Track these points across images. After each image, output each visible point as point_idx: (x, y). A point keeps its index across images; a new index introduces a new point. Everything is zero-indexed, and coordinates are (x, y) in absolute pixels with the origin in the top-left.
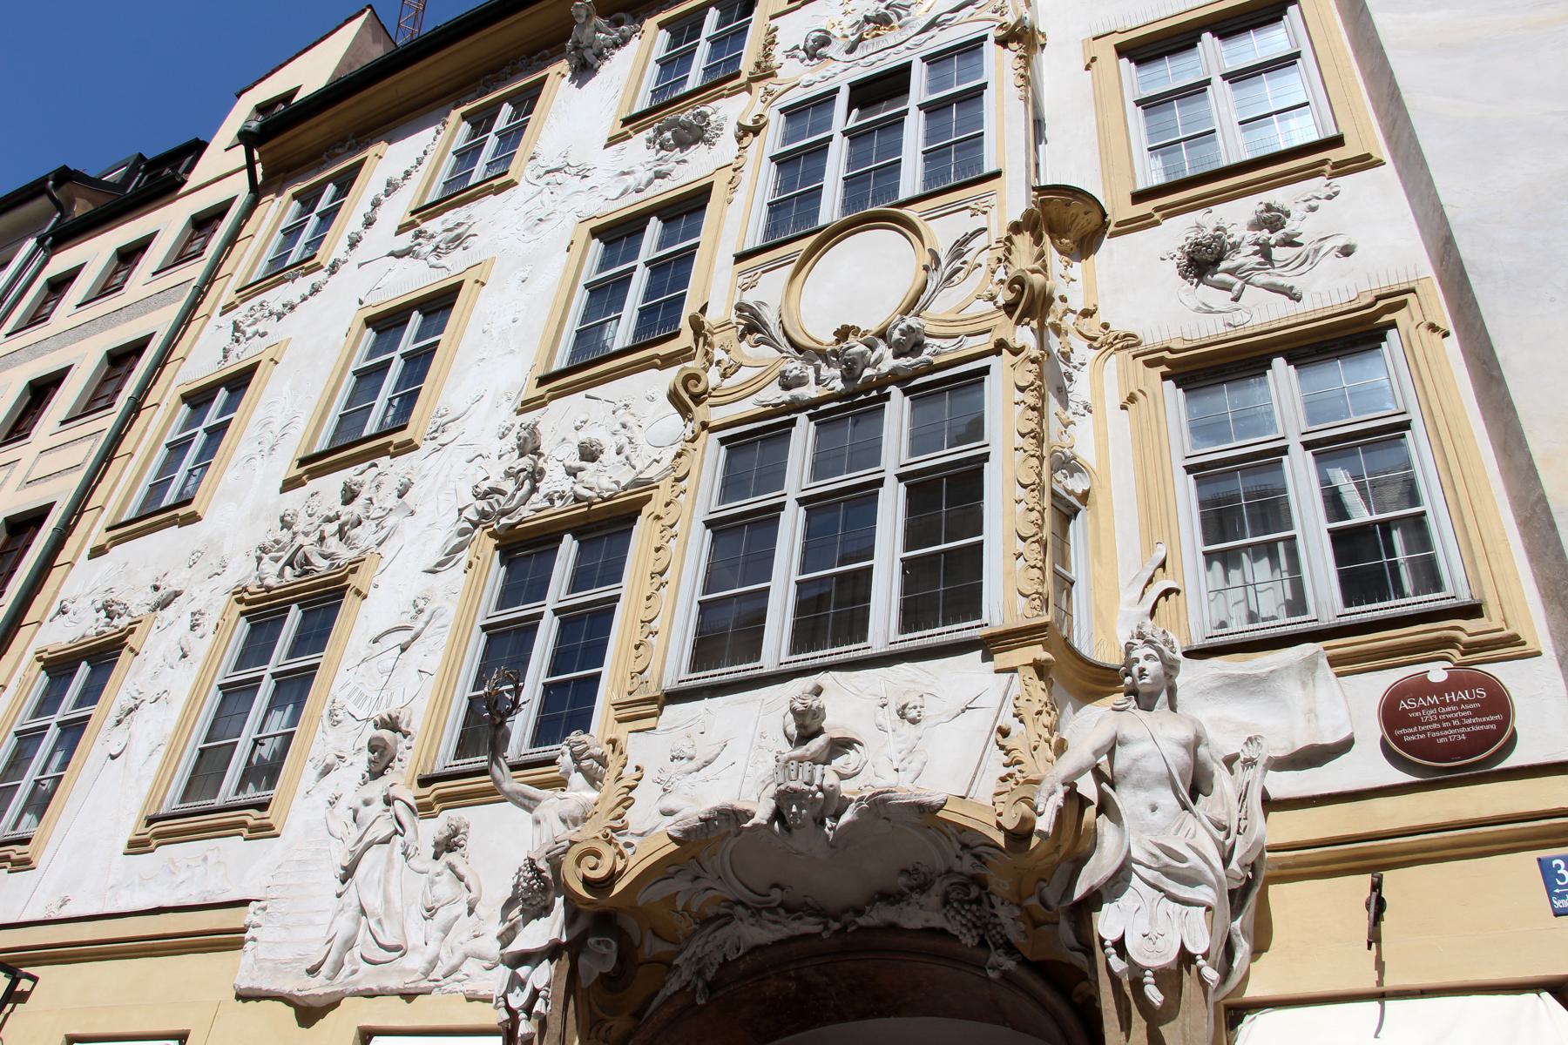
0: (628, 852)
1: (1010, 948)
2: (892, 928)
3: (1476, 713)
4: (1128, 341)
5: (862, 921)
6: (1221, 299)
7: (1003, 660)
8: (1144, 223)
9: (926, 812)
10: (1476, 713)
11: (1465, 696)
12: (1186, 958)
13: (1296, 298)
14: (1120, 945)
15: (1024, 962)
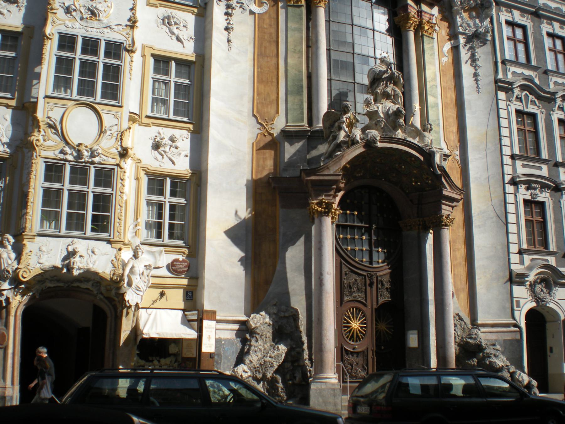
0: (31, 271)
1: (101, 294)
2: (78, 287)
3: (185, 267)
4: (140, 161)
5: (73, 285)
6: (159, 157)
7: (114, 245)
8: (147, 125)
9: (96, 274)
10: (185, 267)
11: (184, 264)
12: (137, 303)
13: (173, 163)
14: (128, 301)
15: (104, 297)
